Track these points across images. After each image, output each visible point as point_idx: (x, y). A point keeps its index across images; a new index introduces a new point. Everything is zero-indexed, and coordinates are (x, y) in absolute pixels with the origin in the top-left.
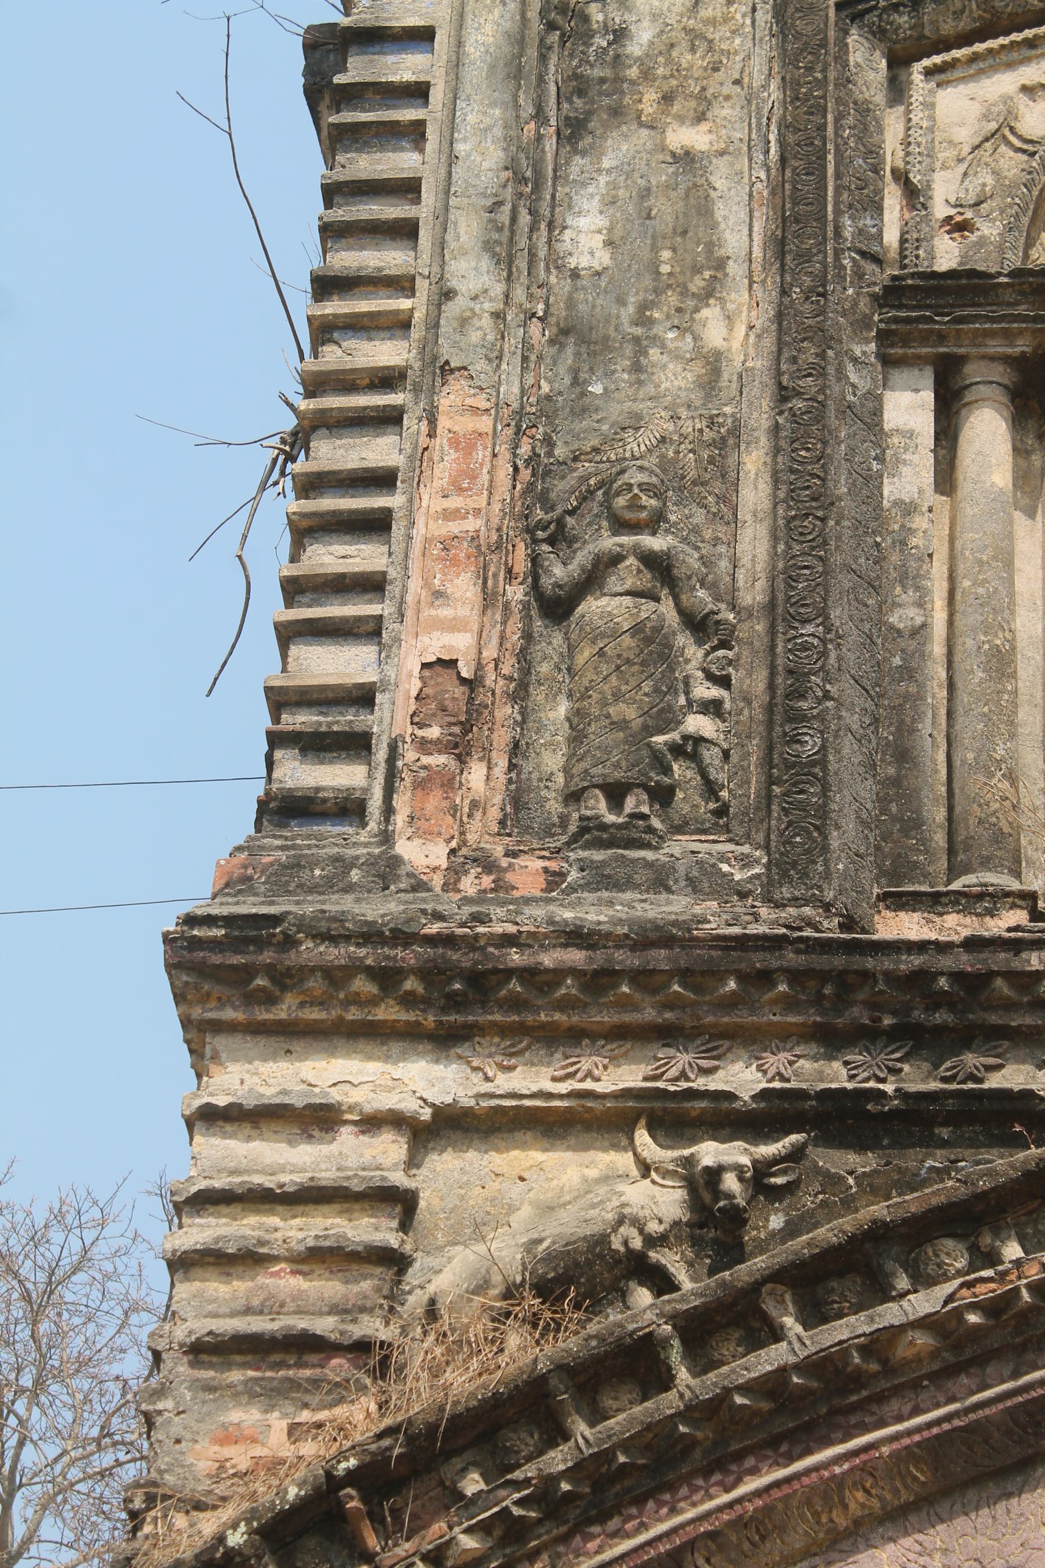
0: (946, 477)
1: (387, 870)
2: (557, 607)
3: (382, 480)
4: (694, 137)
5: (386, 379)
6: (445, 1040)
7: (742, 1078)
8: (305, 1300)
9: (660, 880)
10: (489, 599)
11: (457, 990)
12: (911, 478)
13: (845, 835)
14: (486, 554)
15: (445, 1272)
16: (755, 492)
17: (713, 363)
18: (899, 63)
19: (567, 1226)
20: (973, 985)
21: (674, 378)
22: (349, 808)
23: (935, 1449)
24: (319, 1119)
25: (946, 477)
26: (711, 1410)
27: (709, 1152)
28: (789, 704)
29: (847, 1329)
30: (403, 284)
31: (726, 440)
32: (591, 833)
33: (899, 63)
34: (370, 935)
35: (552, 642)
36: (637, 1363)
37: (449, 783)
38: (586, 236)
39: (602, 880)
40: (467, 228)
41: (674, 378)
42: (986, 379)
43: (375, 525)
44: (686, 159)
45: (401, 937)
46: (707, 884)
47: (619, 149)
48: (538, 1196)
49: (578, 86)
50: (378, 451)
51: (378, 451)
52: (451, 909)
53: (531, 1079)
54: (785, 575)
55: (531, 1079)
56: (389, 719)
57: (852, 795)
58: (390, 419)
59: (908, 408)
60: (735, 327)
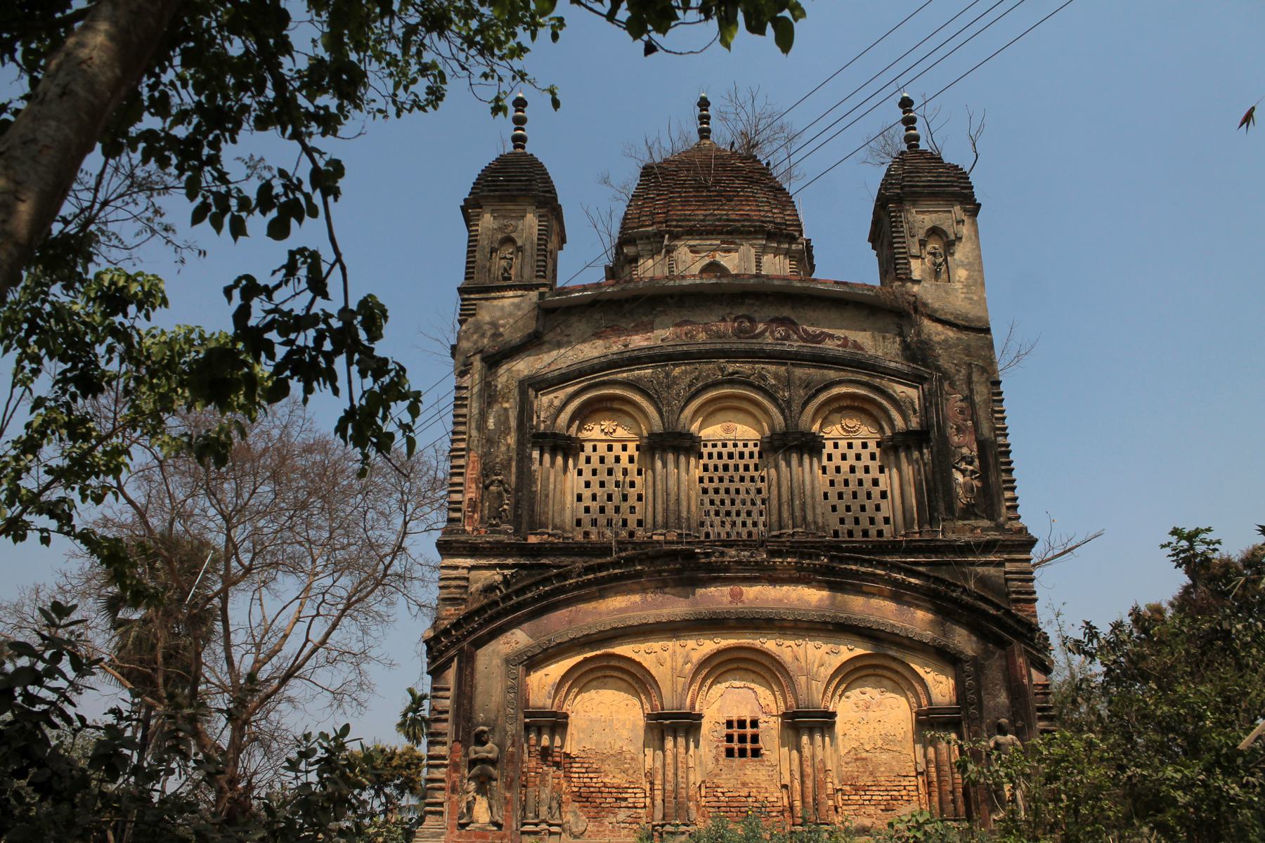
0: (541, 463)
1: (464, 531)
2: (486, 487)
3: (462, 467)
4: (506, 405)
5: (462, 450)
6: (471, 556)
7: (510, 561)
8: (455, 593)
9: (500, 532)
10: (477, 487)
11: (472, 550)
12: (536, 466)
13: (524, 526)
14: (476, 481)
15: (473, 589)
16: (514, 470)
17: (509, 445)
18: (537, 391)
19: (488, 582)
20: (539, 549)
21: (503, 449)
22: (459, 520)
23: (531, 612)
24: (456, 568)
25: (541, 463)
26: (505, 609)
27: (506, 572)
28: (516, 506)
29: (521, 598)
30: (464, 433)
31: (510, 459)
32: (491, 525)
33: (537, 391)
34: (462, 542)
35: (486, 493)
36: (496, 603)
37: (472, 517)
38: (491, 423)
39: (493, 532)
40: (473, 425)
41: (503, 449)
42: (547, 449)
43: (461, 474)
44: (506, 409)
45: (465, 542)
46: (506, 533)
47: (496, 407)
48: (485, 576)
49: (490, 396)
50: (461, 462)
51: (461, 462)
52: (473, 539)
53: (483, 562)
54: (517, 484)
55: (483, 562)
56: (464, 506)
57: (525, 519)
58: (463, 456)
59: (536, 454)
60: (511, 440)
